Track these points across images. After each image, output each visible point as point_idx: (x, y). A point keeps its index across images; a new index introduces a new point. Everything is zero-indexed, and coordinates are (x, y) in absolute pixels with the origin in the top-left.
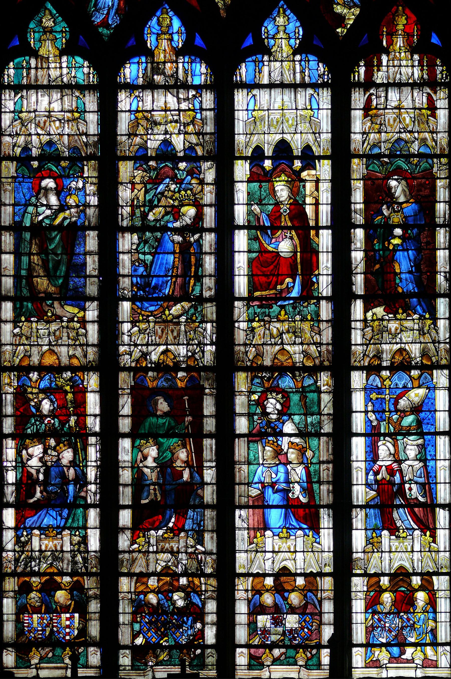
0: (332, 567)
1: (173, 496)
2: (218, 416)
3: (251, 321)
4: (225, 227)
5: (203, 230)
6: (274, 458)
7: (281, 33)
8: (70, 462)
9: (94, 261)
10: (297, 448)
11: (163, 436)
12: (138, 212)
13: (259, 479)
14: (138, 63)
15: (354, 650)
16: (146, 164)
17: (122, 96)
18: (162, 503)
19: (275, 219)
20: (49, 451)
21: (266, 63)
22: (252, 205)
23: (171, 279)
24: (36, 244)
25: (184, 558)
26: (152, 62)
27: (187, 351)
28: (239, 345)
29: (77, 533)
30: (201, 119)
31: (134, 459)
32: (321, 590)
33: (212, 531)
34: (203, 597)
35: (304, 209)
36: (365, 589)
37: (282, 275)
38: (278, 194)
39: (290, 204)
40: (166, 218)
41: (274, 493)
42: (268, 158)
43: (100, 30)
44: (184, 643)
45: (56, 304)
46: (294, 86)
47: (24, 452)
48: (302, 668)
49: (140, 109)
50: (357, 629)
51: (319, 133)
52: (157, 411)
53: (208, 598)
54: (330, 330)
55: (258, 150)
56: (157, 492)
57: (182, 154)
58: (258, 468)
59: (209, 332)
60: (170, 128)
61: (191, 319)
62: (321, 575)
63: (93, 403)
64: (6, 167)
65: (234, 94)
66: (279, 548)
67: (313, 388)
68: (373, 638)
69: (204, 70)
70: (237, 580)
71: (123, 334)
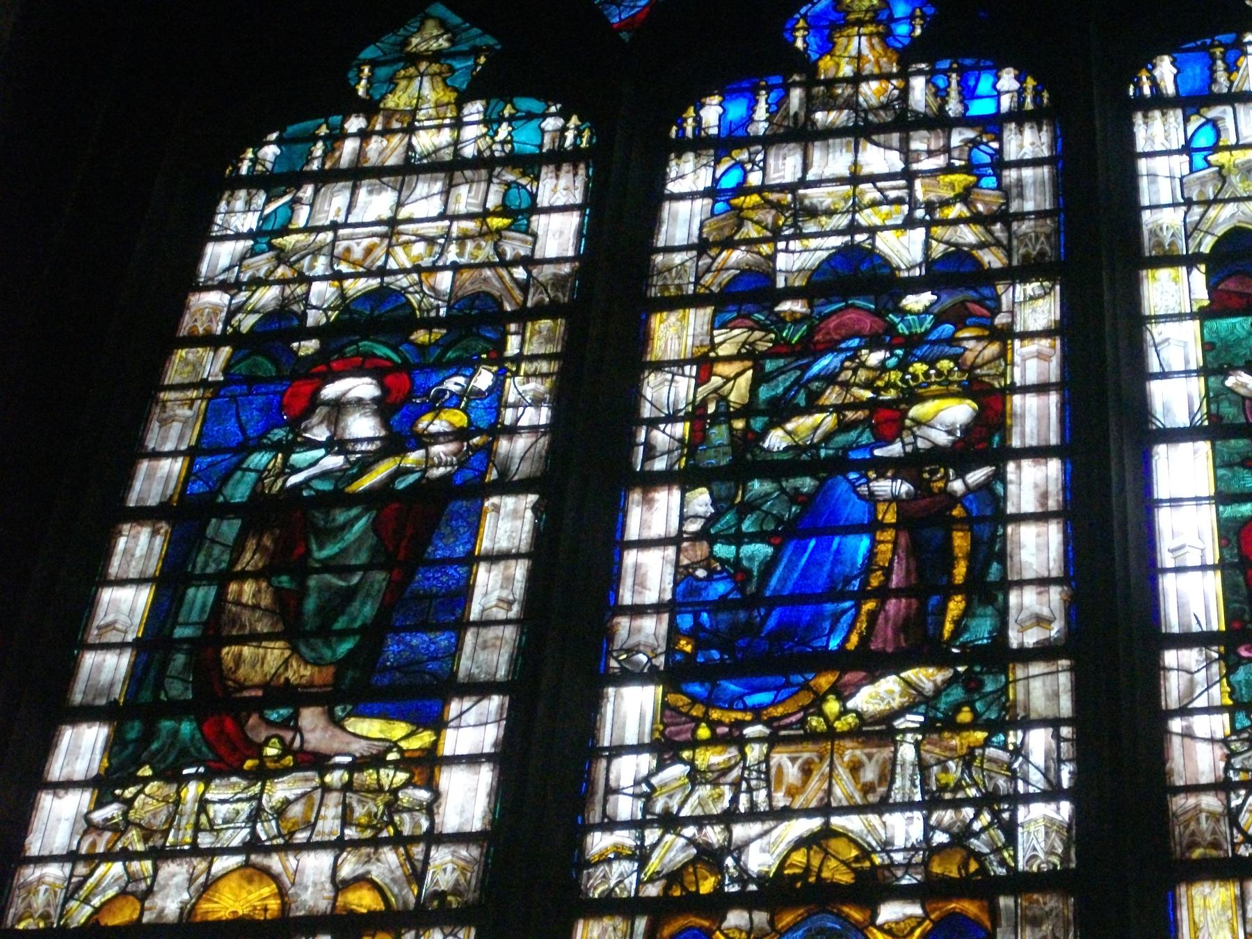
9: (508, 581)
12: (719, 434)
24: (259, 548)
26: (807, 85)
27: (928, 829)
45: (310, 718)
64: (185, 362)
65: (1132, 124)
69: (1008, 80)
71: (611, 791)
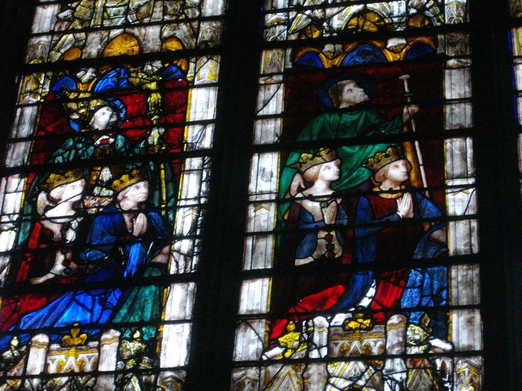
1: (373, 248)
8: (140, 204)
11: (351, 143)
20: (96, 191)
25: (399, 368)
29: (137, 335)
33: (470, 307)
47: (42, 196)
52: (339, 103)
56: (335, 242)
63: (202, 104)
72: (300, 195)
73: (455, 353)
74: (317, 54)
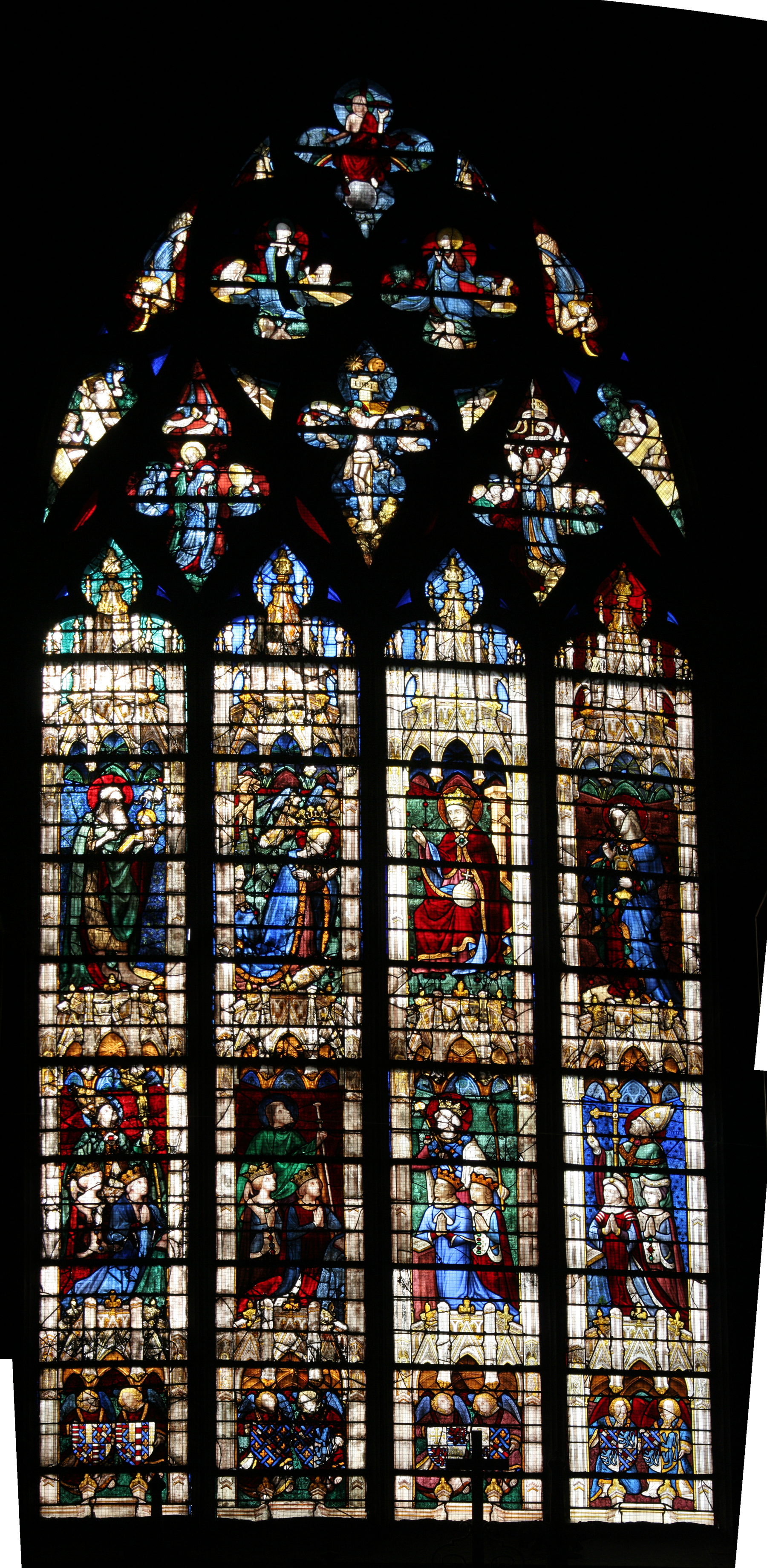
0: (538, 1357)
2: (365, 1132)
3: (413, 995)
4: (374, 860)
5: (342, 863)
6: (450, 1196)
7: (453, 592)
10: (484, 1182)
11: (283, 1160)
12: (244, 835)
13: (429, 1226)
14: (244, 624)
15: (573, 1481)
16: (257, 767)
17: (220, 671)
18: (281, 1258)
19: (447, 852)
21: (431, 632)
22: (413, 830)
23: (294, 932)
27: (319, 1036)
28: (397, 1029)
30: (337, 706)
31: (240, 1192)
32: (523, 1392)
33: (358, 1301)
34: (345, 1398)
35: (490, 840)
36: (588, 1392)
37: (459, 932)
38: (452, 817)
39: (470, 832)
40: (287, 844)
41: (450, 1247)
42: (437, 765)
43: (188, 577)
44: (316, 1466)
46: (472, 668)
48: (495, 1507)
49: (247, 688)
50: (576, 1450)
51: (510, 735)
52: (273, 1123)
53: (353, 1401)
54: (530, 1014)
55: (422, 754)
56: (275, 1242)
57: (309, 754)
58: (426, 1208)
59: (351, 1009)
60: (292, 716)
61: (324, 990)
62: (523, 1369)
65: (385, 674)
66: (459, 1328)
67: (506, 1096)
68: (600, 1464)
69: (340, 637)
70: (396, 1373)
71: (222, 1010)
72: (250, 1201)
73: (348, 1333)
74: (256, 1073)
